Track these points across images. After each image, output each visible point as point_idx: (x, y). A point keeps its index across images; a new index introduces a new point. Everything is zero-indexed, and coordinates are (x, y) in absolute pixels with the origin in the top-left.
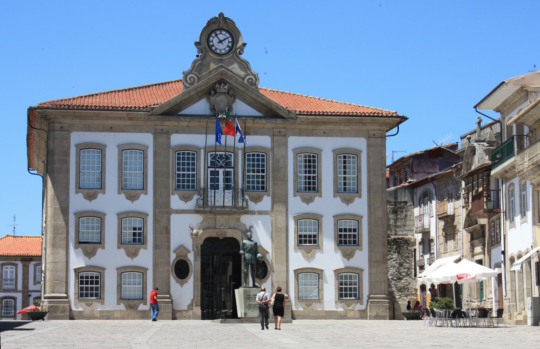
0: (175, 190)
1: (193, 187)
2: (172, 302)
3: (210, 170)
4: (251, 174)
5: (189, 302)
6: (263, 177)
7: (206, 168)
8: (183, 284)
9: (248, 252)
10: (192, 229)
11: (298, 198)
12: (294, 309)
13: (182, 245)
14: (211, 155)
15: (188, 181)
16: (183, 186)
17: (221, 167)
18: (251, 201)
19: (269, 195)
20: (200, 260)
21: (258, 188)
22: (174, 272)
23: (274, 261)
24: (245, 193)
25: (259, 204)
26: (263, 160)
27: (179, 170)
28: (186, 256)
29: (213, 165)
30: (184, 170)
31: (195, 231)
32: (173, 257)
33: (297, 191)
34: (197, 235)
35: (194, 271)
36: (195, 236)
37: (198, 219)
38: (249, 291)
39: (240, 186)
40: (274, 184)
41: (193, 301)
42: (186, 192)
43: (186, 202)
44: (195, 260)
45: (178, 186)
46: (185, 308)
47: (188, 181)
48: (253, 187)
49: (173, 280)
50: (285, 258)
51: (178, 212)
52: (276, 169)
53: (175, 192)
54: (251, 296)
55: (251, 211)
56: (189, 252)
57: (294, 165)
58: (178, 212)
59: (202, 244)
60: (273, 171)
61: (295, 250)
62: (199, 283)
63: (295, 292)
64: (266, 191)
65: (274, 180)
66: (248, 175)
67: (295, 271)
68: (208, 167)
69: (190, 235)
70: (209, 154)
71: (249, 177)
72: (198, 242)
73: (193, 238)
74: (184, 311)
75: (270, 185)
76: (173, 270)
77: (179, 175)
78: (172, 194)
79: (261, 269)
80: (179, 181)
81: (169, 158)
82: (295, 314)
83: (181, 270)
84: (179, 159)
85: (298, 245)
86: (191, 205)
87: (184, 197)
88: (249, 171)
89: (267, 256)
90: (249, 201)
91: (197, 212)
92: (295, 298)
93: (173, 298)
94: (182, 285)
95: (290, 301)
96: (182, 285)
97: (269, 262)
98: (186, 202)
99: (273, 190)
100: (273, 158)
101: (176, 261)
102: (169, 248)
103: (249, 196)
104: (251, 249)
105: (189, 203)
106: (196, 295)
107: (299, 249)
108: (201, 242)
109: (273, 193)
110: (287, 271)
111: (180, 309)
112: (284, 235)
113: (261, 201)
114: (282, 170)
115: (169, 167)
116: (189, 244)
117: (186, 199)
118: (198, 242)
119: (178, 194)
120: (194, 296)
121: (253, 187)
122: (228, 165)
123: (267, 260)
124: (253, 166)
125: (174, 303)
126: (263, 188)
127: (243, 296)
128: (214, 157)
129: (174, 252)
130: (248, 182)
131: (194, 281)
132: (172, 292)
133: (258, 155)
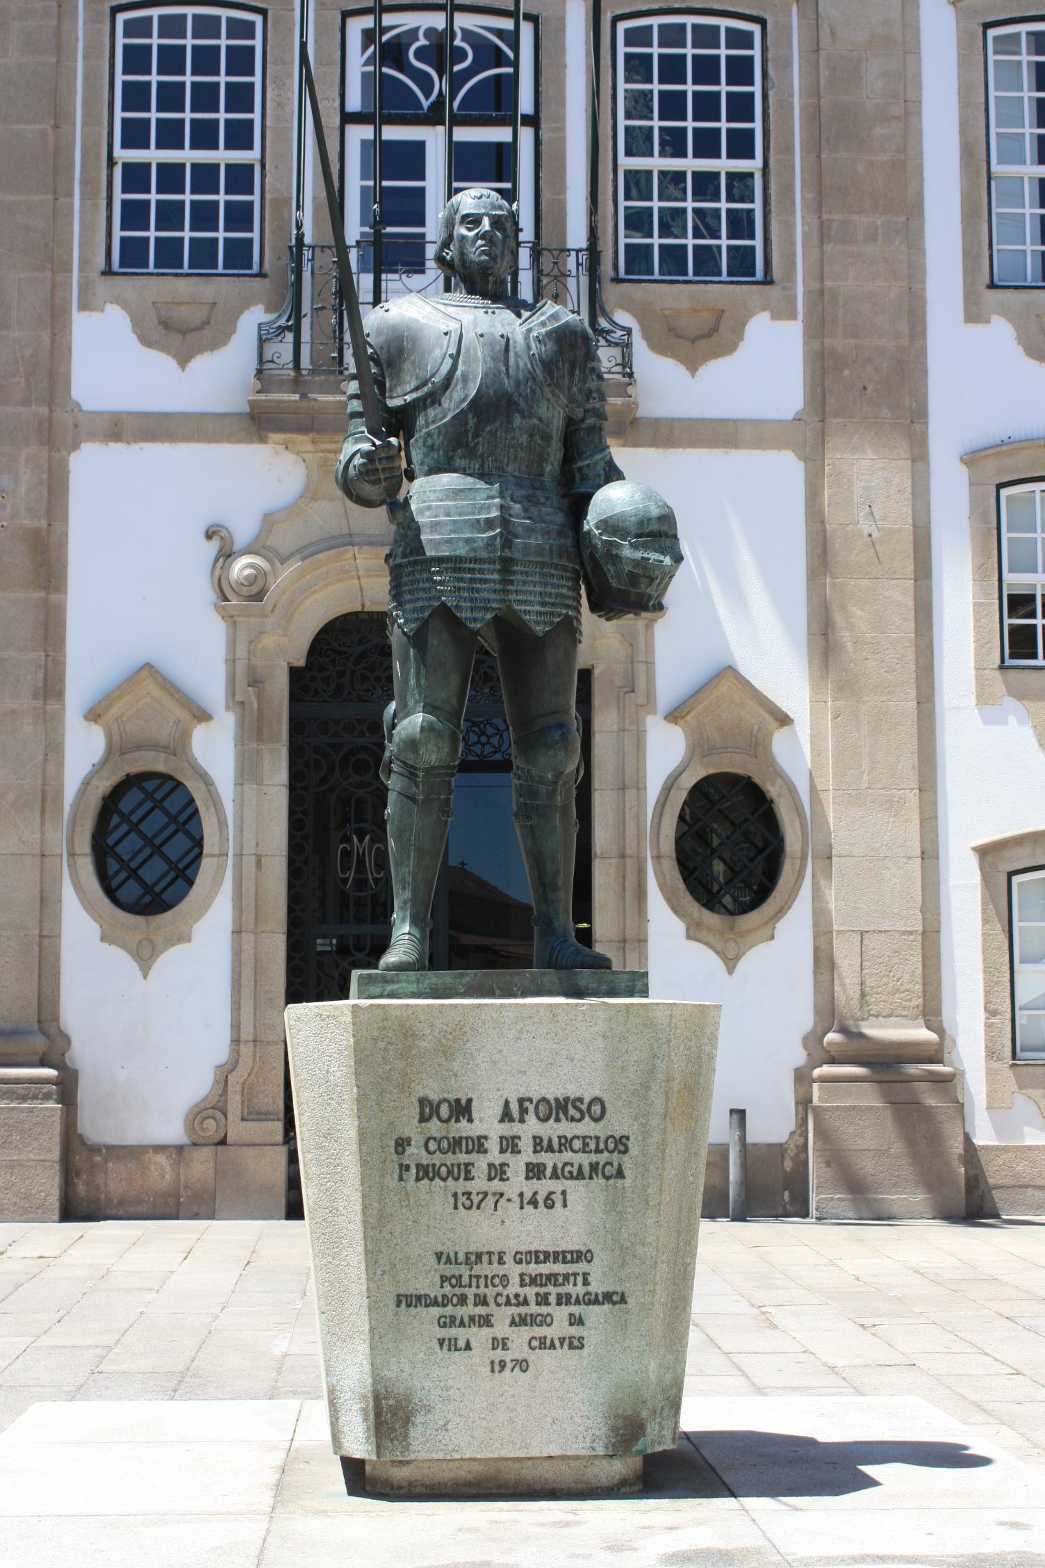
0: (108, 272)
1: (239, 255)
2: (66, 1089)
3: (359, 134)
4: (657, 163)
5: (196, 1084)
6: (740, 183)
7: (332, 120)
8: (155, 953)
9: (457, 450)
10: (227, 554)
11: (1000, 333)
12: (984, 1137)
13: (148, 666)
14: (368, 37)
15: (205, 215)
16: (169, 254)
17: (433, 117)
18: (659, 346)
19: (785, 312)
20: (283, 776)
21: (706, 261)
22: (87, 865)
23: (827, 782)
24: (611, 293)
25: (714, 369)
26: (741, 70)
27: (135, 135)
28: (179, 746)
29: (389, 103)
30: (170, 136)
31: (241, 567)
32: (83, 753)
33: (989, 282)
34: (256, 592)
35: (239, 856)
36: (240, 601)
37: (263, 480)
38: (451, 1044)
39: (577, 236)
40: (823, 234)
41: (224, 1075)
42: (184, 290)
43: (183, 361)
44: (247, 771)
45: (133, 254)
46: (172, 1131)
47: (205, 215)
48: (674, 258)
49: (80, 922)
50: (908, 763)
51: (122, 428)
52: (833, 126)
53: (104, 286)
54: (486, 1122)
55: (656, 422)
56: (203, 716)
57: (964, 103)
58: (122, 428)
59: (301, 662)
60: (815, 145)
61: (984, 697)
62: (277, 946)
63: (991, 1012)
64: (768, 281)
65: (818, 205)
66: (632, 175)
67: (984, 852)
68: (348, 118)
69: (210, 595)
70: (357, 26)
71: (637, 183)
72: (269, 641)
73: (231, 619)
74: (159, 1148)
75: (794, 234)
76: (84, 844)
77: (136, 176)
78: (84, 306)
79: (735, 846)
80: (134, 215)
81: (61, 48)
82: (995, 1174)
83: (143, 846)
84: (136, 59)
85: (1002, 667)
86: (220, 376)
87: (166, 324)
88: (638, 143)
89: (780, 743)
90: (640, 346)
91: (258, 423)
92: (991, 1054)
93: (82, 1053)
94: (145, 958)
95: (946, 1083)
96: (145, 958)
97: (792, 790)
98: (183, 361)
99: (819, 271)
100: (814, 48)
101: (104, 786)
102: (51, 687)
103: (643, 314)
104: (493, 407)
105: (201, 363)
106: (247, 1033)
107: (1019, 695)
108: (293, 644)
109: (819, 298)
110: (930, 855)
111: (132, 1137)
112: (901, 595)
113: (728, 348)
114: (879, 131)
115: (60, 116)
116: (201, 654)
117: (180, 336)
118: (269, 641)
119: (123, 304)
120: (236, 1041)
121: (674, 258)
122: (496, 101)
123: (779, 774)
124: (672, 106)
125: (84, 1094)
126: (742, 263)
127: (350, 1132)
128: (392, 52)
129: (93, 715)
130: (638, 222)
131: (237, 932)
132: (74, 1013)
133: (706, 36)
